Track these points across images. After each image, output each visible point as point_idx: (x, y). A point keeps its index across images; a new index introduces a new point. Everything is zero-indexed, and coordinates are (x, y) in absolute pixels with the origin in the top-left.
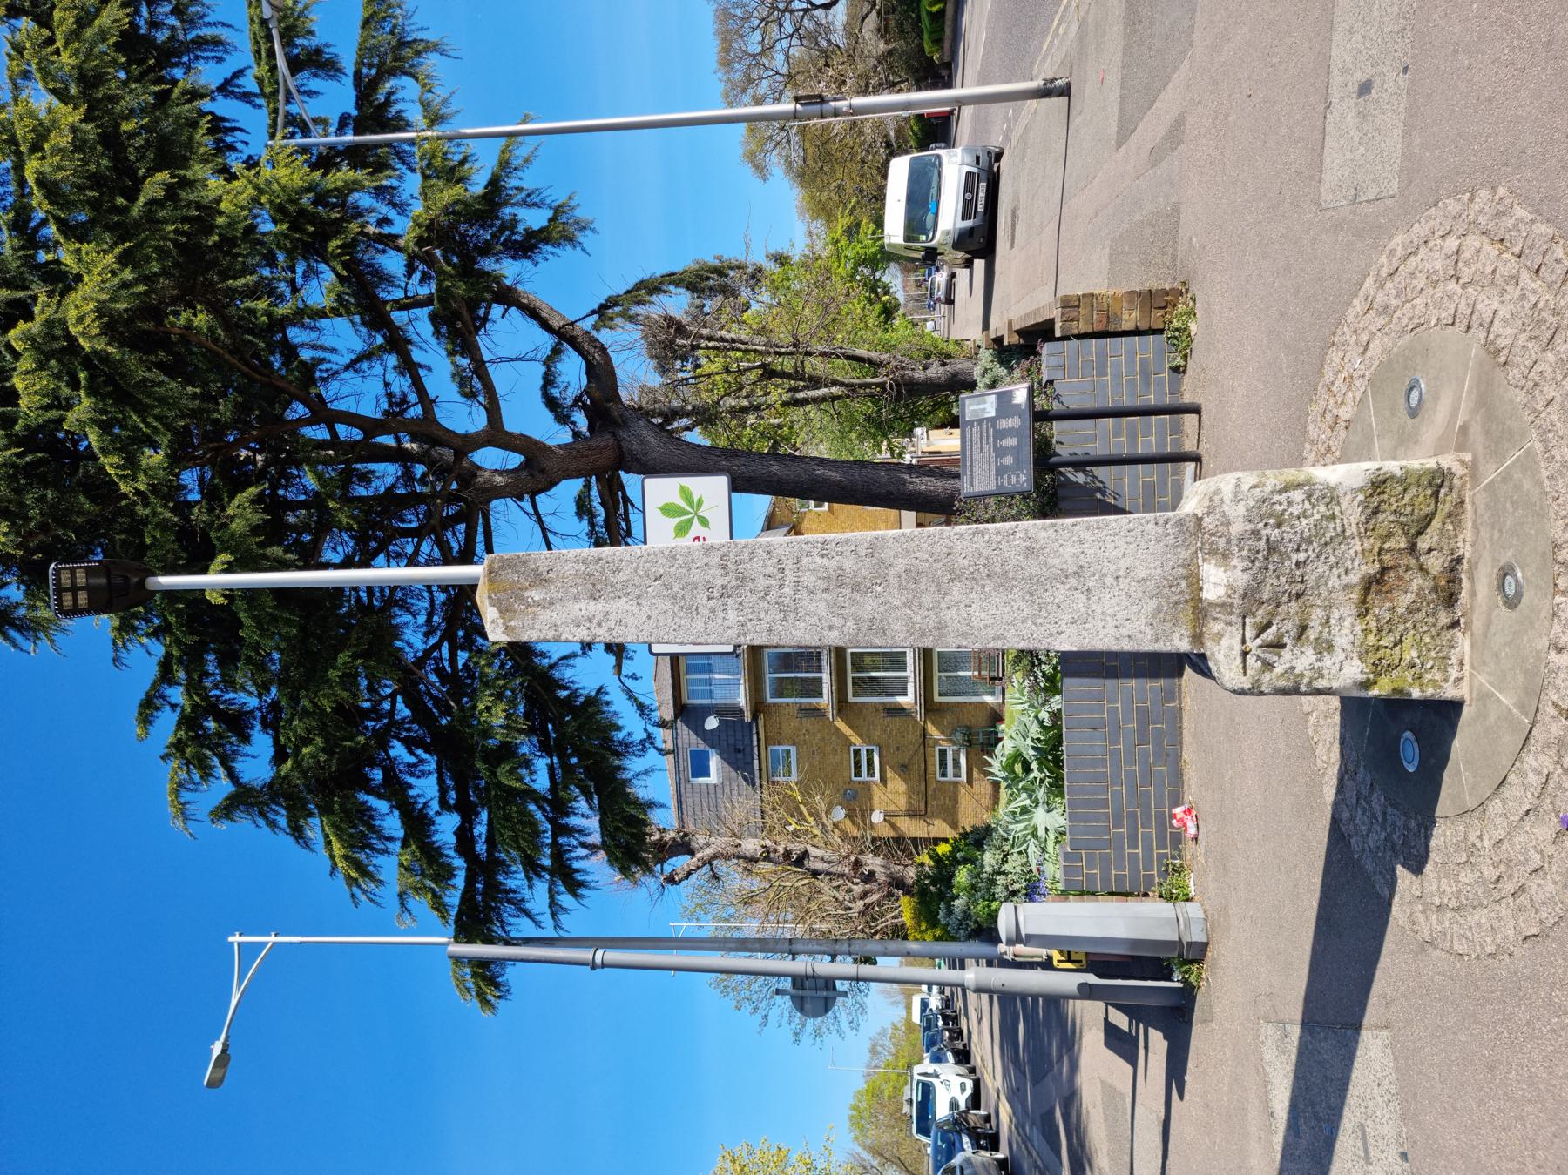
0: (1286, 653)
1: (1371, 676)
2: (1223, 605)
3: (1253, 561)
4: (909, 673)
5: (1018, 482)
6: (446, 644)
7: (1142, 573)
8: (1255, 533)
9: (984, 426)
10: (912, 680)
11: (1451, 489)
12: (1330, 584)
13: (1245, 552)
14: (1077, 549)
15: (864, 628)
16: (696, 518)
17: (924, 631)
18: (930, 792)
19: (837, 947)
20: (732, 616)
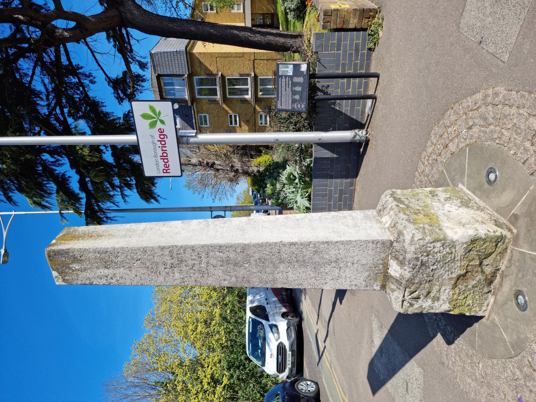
0: (420, 301)
1: (452, 309)
2: (397, 280)
3: (414, 269)
4: (249, 86)
5: (301, 107)
6: (58, 108)
7: (364, 262)
8: (417, 259)
9: (287, 79)
10: (250, 89)
11: (503, 243)
12: (444, 277)
13: (411, 265)
14: (337, 252)
15: (240, 280)
16: (158, 120)
20: (177, 275)
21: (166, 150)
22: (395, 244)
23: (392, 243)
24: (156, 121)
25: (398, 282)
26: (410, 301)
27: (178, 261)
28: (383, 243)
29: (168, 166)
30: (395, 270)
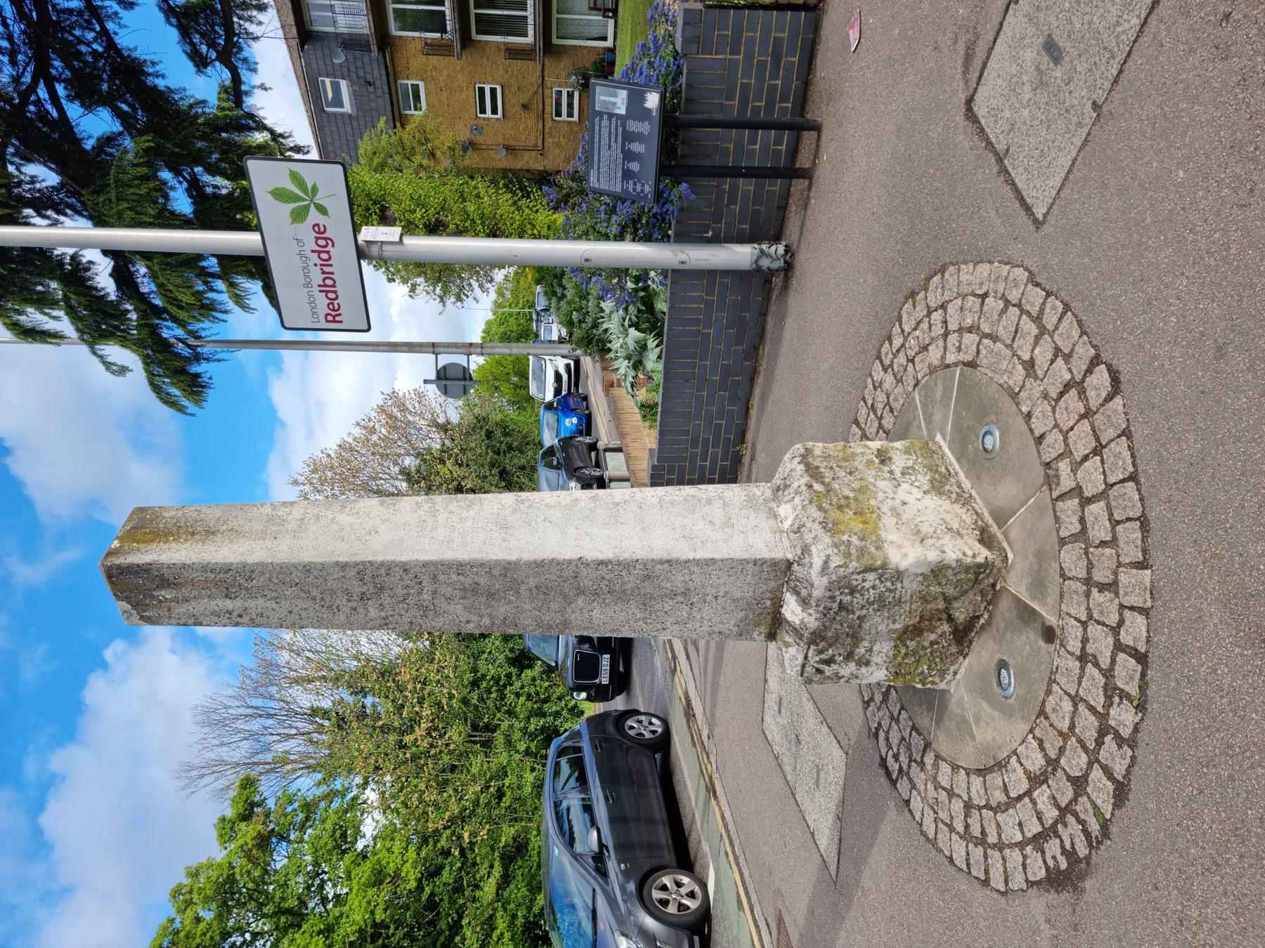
2: (796, 629)
4: (529, 13)
7: (738, 595)
8: (832, 598)
9: (614, 123)
10: (530, 21)
11: (989, 575)
13: (821, 609)
16: (312, 205)
17: (551, 626)
18: (547, 131)
19: (472, 350)
21: (332, 273)
22: (795, 567)
23: (789, 564)
24: (307, 208)
25: (796, 631)
26: (816, 665)
27: (375, 587)
28: (774, 564)
29: (336, 307)
30: (792, 610)
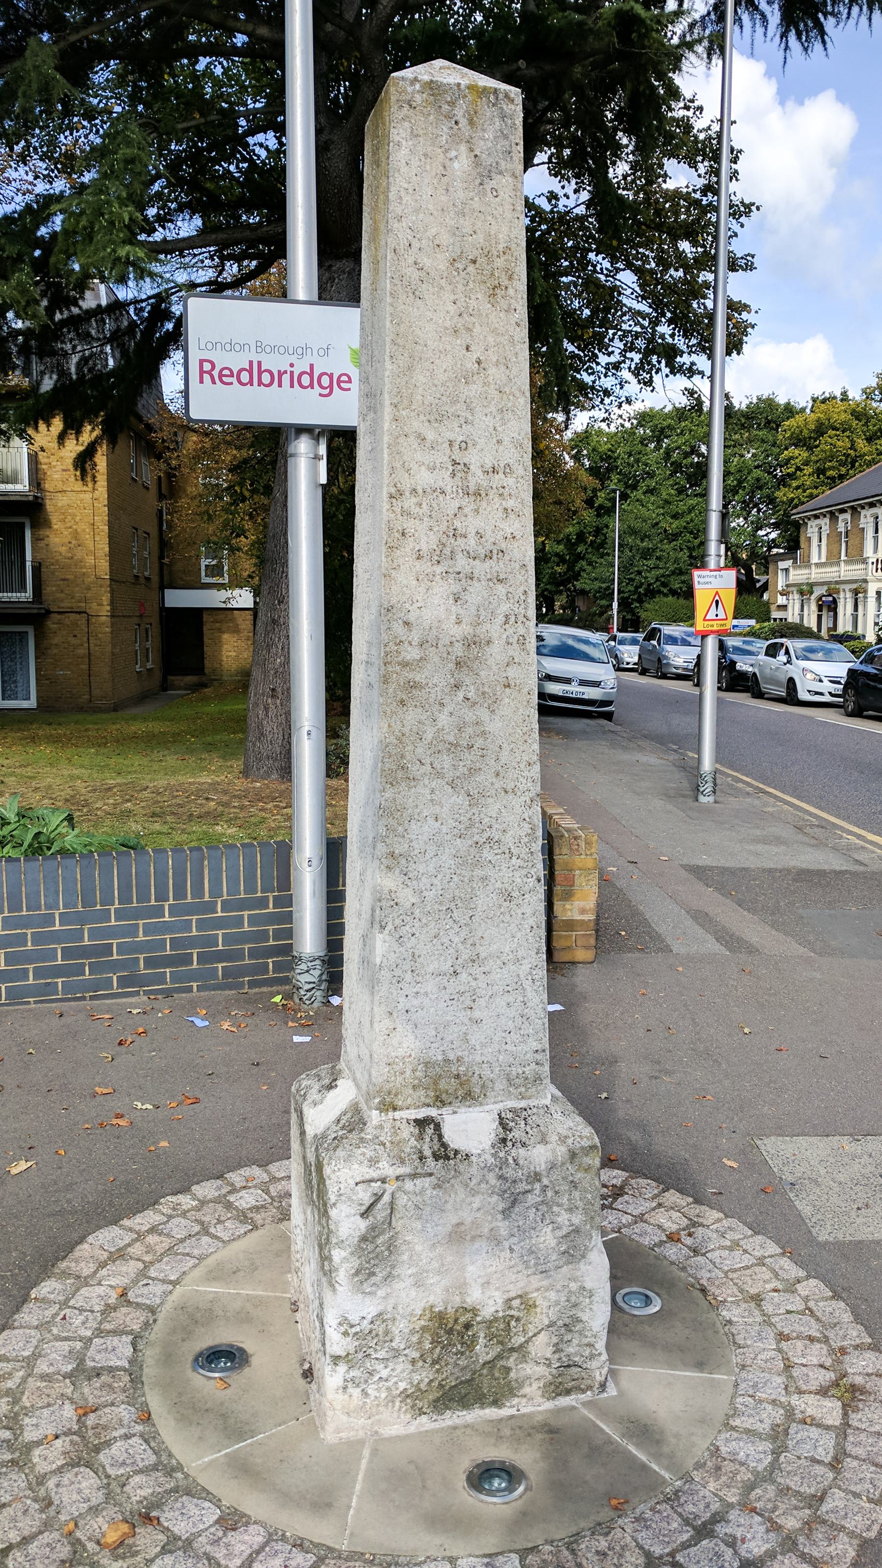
7: (475, 1039)
21: (280, 385)
